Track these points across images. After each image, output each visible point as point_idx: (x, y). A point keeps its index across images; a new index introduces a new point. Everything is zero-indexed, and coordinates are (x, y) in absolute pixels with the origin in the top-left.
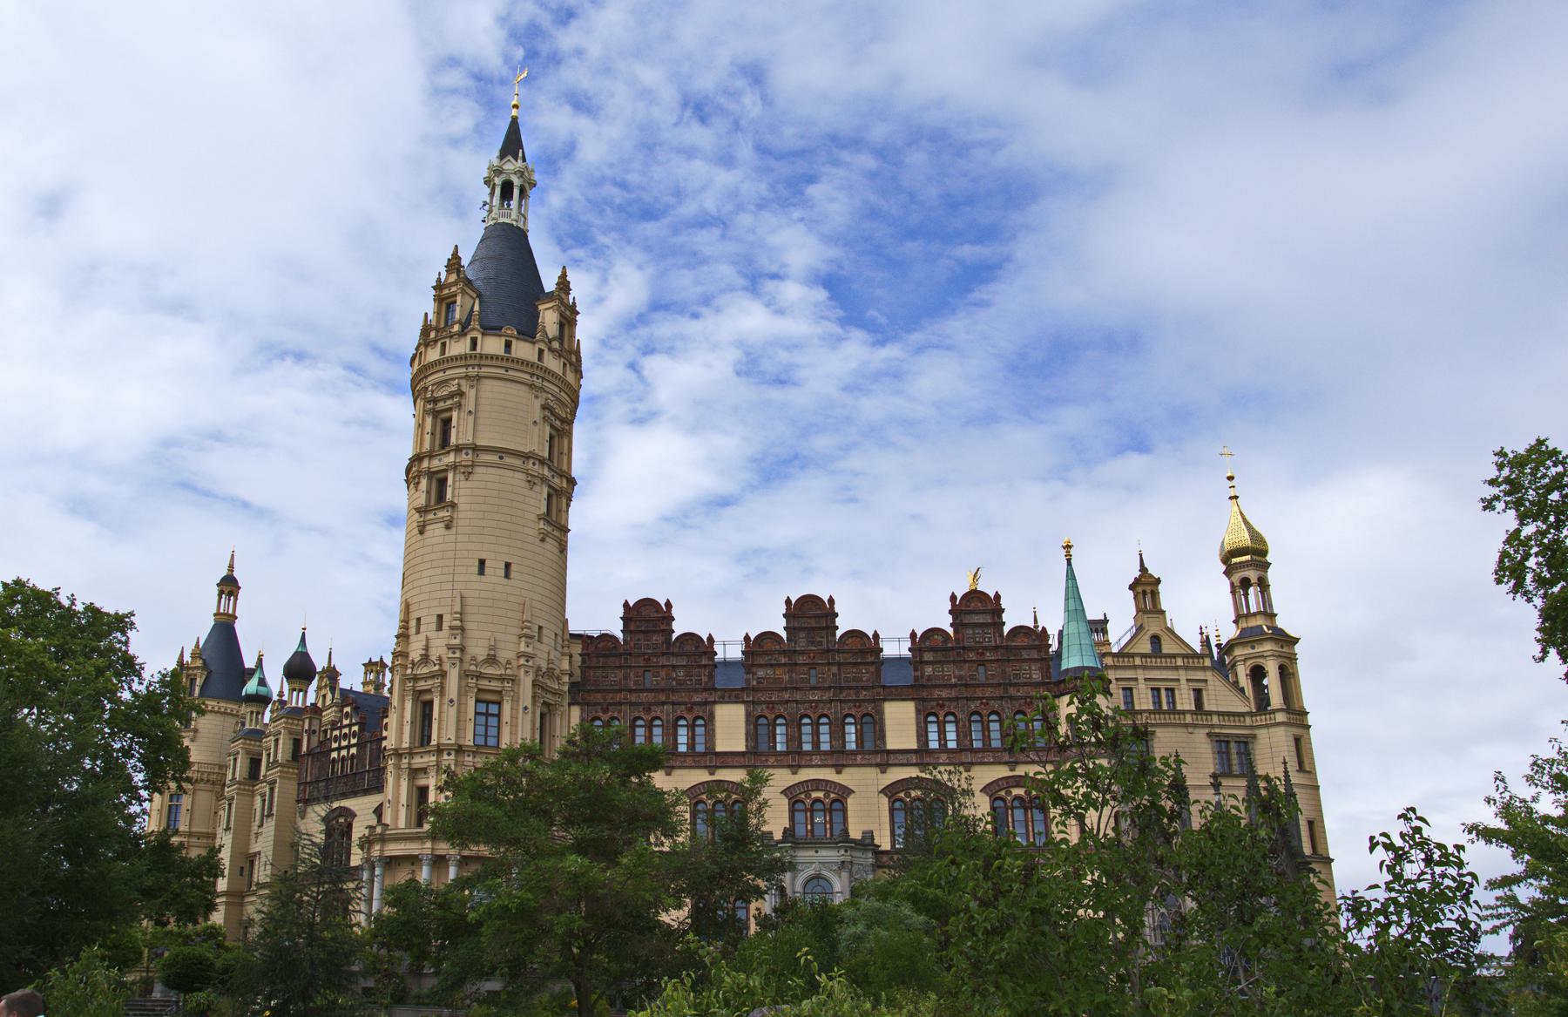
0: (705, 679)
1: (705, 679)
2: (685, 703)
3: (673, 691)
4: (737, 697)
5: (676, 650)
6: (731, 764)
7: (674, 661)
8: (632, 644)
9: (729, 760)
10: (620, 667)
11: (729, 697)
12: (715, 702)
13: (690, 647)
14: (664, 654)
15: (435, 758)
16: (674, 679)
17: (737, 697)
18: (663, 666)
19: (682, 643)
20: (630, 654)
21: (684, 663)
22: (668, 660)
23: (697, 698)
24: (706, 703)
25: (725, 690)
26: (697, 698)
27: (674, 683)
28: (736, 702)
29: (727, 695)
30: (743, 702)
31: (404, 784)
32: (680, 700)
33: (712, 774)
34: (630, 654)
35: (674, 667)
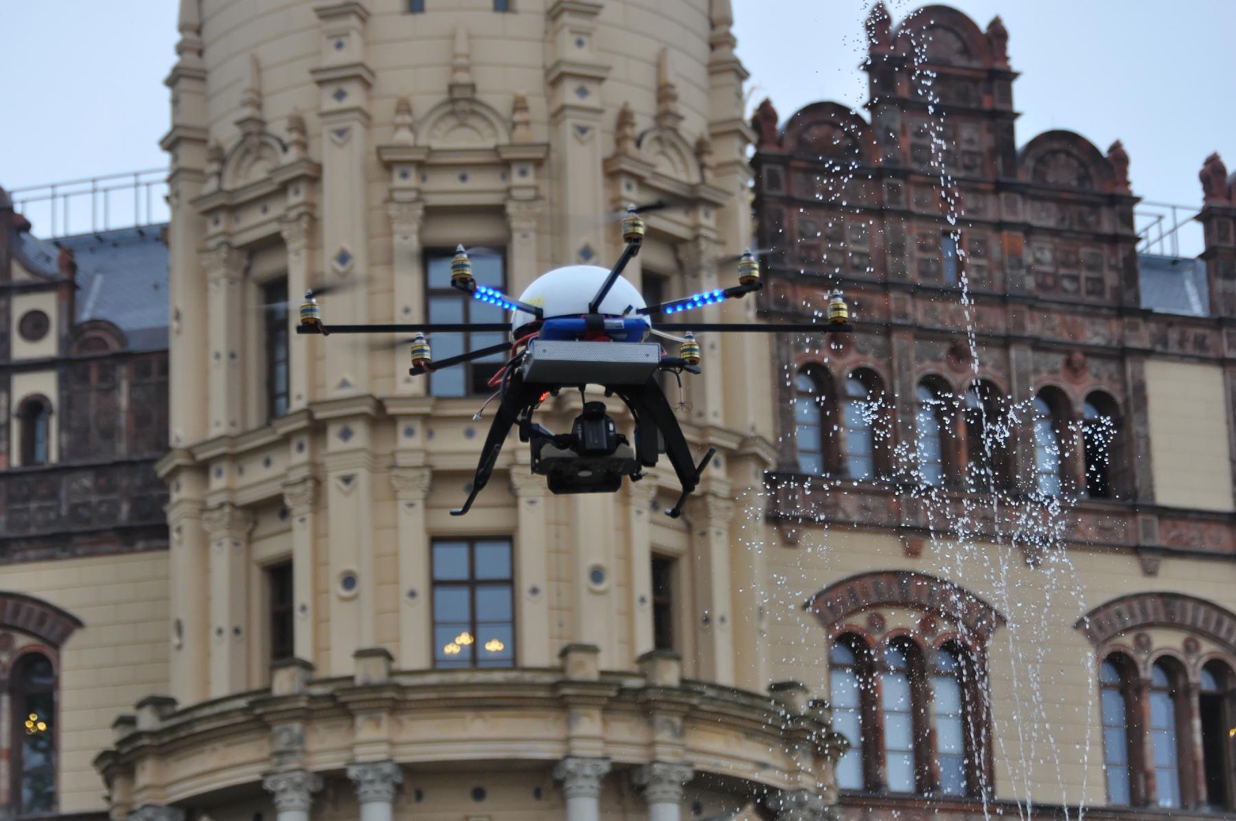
0: (1111, 279)
1: (1111, 279)
2: (1066, 349)
3: (1032, 303)
4: (1200, 343)
5: (1024, 177)
6: (1196, 546)
7: (1026, 213)
8: (905, 143)
9: (1191, 534)
10: (879, 213)
11: (1181, 343)
12: (1147, 353)
13: (1062, 175)
14: (999, 187)
15: (303, 457)
16: (1029, 270)
17: (1200, 343)
18: (1000, 226)
19: (1040, 160)
20: (905, 174)
21: (1051, 223)
22: (1012, 208)
23: (1095, 334)
24: (1120, 354)
25: (1169, 320)
26: (1095, 334)
27: (1030, 282)
28: (1203, 360)
29: (1174, 335)
30: (1223, 362)
31: (222, 559)
32: (1048, 335)
33: (1150, 572)
34: (905, 174)
35: (1029, 230)
